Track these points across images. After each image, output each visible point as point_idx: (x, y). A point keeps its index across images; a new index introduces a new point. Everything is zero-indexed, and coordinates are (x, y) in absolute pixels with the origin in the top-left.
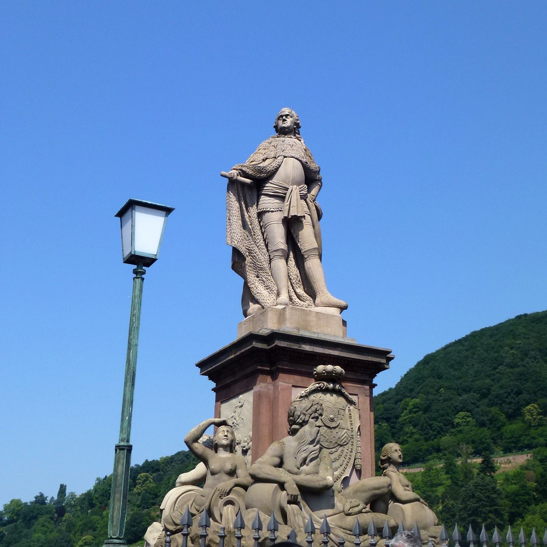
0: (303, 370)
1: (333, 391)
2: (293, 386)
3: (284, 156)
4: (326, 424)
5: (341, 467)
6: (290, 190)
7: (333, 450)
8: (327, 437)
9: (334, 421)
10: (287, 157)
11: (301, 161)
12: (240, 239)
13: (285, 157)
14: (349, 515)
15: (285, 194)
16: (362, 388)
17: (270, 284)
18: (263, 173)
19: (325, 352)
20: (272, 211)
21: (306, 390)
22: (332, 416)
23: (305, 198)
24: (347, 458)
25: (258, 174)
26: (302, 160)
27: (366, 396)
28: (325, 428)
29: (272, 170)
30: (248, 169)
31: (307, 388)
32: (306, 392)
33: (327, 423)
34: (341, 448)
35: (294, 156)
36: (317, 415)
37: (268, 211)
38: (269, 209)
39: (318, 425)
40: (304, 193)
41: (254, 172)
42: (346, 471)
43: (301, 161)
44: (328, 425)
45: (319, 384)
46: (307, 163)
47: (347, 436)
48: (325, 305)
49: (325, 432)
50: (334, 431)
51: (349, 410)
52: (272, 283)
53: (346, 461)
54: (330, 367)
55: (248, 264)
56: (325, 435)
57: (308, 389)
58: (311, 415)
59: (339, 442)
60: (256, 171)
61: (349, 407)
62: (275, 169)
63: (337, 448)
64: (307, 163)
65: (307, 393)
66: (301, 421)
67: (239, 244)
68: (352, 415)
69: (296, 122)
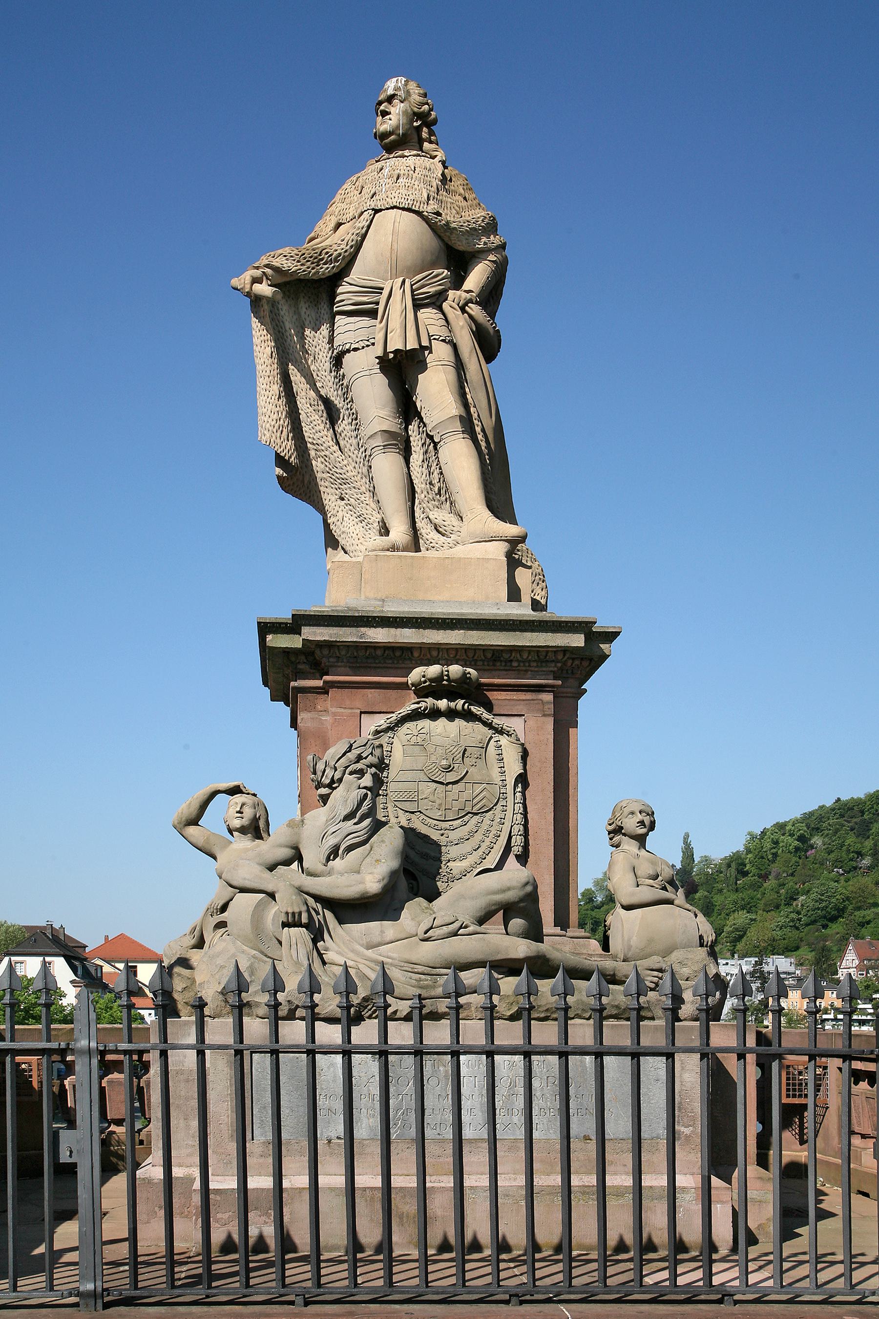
1: (451, 714)
12: (277, 426)
15: (377, 303)
16: (535, 702)
17: (364, 511)
18: (325, 264)
20: (356, 350)
25: (313, 268)
27: (544, 715)
37: (348, 351)
38: (347, 346)
41: (302, 265)
66: (327, 781)
67: (274, 437)
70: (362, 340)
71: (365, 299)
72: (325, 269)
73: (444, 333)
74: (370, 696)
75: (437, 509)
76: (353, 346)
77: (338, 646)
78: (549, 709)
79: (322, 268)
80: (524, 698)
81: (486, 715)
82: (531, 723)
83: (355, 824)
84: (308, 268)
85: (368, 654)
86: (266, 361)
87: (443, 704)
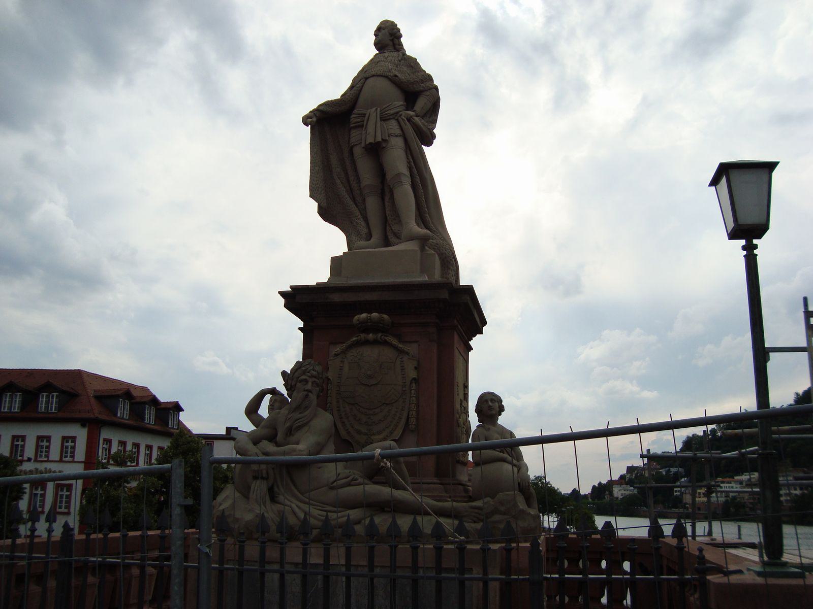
1: (375, 342)
3: (365, 78)
4: (363, 382)
6: (367, 116)
11: (386, 77)
13: (366, 79)
14: (332, 488)
15: (363, 121)
20: (356, 145)
22: (369, 373)
31: (344, 343)
36: (303, 377)
39: (306, 389)
40: (391, 112)
43: (386, 77)
45: (357, 337)
46: (396, 76)
54: (364, 315)
58: (299, 377)
69: (390, 32)
71: (359, 120)
73: (398, 132)
76: (355, 143)
81: (395, 342)
83: (300, 413)
87: (371, 336)
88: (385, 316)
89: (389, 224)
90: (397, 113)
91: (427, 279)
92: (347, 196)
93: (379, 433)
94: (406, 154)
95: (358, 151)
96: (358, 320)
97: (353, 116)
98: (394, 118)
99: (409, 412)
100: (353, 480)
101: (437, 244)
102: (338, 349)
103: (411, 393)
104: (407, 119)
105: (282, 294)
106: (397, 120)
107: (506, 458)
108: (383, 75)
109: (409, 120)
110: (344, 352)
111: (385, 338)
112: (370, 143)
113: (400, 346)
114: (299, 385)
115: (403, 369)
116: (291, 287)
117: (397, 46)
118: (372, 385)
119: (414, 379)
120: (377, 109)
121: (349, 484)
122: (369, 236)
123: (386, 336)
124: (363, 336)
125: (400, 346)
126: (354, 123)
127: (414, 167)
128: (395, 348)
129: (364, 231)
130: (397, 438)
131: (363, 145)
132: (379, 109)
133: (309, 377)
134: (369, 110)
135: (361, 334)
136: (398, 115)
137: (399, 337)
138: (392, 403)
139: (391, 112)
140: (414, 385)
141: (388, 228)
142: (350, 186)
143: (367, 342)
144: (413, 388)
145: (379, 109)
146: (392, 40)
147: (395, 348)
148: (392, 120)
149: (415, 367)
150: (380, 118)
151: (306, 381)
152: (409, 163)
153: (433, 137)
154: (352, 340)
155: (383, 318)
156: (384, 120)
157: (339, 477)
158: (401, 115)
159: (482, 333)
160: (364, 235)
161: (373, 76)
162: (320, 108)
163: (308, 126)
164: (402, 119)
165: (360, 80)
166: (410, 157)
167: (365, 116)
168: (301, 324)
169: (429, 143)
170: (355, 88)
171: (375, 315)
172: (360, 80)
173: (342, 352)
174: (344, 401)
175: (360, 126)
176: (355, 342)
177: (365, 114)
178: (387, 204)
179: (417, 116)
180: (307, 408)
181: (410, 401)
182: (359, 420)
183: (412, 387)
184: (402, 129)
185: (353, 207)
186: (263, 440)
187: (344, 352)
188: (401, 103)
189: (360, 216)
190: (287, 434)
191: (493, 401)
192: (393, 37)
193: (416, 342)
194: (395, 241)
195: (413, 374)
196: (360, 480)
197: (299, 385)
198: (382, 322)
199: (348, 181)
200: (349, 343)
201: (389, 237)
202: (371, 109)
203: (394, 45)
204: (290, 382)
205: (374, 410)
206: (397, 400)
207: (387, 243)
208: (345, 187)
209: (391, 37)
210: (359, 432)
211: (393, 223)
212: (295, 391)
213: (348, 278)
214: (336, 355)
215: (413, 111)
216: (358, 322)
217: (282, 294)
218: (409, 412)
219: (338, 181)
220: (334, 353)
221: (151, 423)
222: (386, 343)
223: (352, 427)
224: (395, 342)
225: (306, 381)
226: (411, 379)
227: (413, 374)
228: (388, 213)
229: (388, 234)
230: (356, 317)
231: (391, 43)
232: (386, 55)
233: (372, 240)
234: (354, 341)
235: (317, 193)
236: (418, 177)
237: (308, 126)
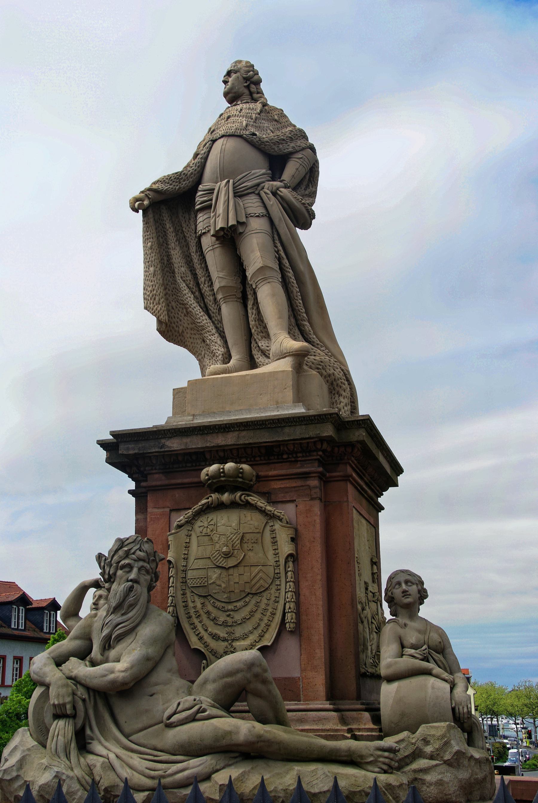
0: (186, 481)
1: (234, 505)
2: (171, 511)
3: (211, 140)
4: (217, 564)
5: (255, 632)
7: (239, 604)
8: (223, 585)
9: (231, 556)
10: (216, 140)
11: (240, 136)
12: (151, 295)
13: (214, 141)
14: (170, 726)
15: (211, 200)
16: (305, 488)
18: (184, 181)
19: (208, 445)
20: (204, 233)
21: (186, 514)
22: (225, 549)
23: (257, 192)
24: (268, 614)
25: (177, 186)
26: (242, 133)
27: (312, 499)
28: (218, 571)
29: (195, 170)
30: (162, 183)
31: (190, 509)
32: (186, 516)
33: (219, 562)
34: (257, 598)
35: (225, 134)
36: (127, 561)
39: (130, 578)
41: (171, 185)
42: (267, 636)
43: (240, 136)
44: (220, 565)
45: (208, 498)
46: (254, 134)
47: (264, 576)
48: (278, 357)
49: (219, 578)
50: (235, 573)
51: (273, 531)
52: (216, 345)
53: (265, 620)
54: (214, 467)
55: (188, 327)
56: (218, 582)
57: (190, 512)
59: (248, 590)
60: (174, 182)
61: (272, 526)
62: (198, 167)
63: (247, 599)
64: (255, 135)
65: (188, 518)
68: (278, 539)
69: (244, 76)
70: (207, 227)
71: (205, 199)
72: (185, 184)
73: (261, 210)
74: (177, 495)
75: (264, 339)
76: (203, 231)
77: (150, 457)
78: (315, 493)
79: (182, 184)
80: (294, 485)
82: (301, 507)
83: (123, 615)
84: (174, 186)
85: (172, 460)
86: (148, 252)
87: (226, 497)
88: (246, 467)
89: (255, 340)
90: (258, 185)
91: (303, 410)
92: (195, 305)
93: (245, 637)
94: (274, 240)
95: (207, 242)
96: (207, 475)
97: (199, 193)
98: (253, 193)
99: (285, 604)
100: (198, 712)
101: (321, 362)
102: (181, 518)
103: (286, 577)
104: (272, 193)
105: (103, 444)
106: (259, 195)
107: (431, 670)
108: (236, 134)
109: (274, 194)
110: (190, 522)
111: (246, 498)
112: (222, 229)
113: (269, 508)
114: (120, 572)
115: (274, 542)
116: (113, 434)
117: (255, 96)
118: (230, 568)
119: (291, 555)
120: (228, 182)
121: (193, 719)
122: (227, 357)
123: (248, 495)
124: (214, 496)
125: (269, 508)
126: (199, 204)
127: (285, 257)
128: (263, 512)
129: (220, 351)
130: (269, 644)
131: (212, 232)
132: (231, 181)
133: (135, 560)
134: (219, 184)
135: (212, 495)
136: (260, 188)
137: (267, 496)
138: (261, 592)
139: (249, 184)
140: (291, 564)
141: (253, 344)
142: (200, 290)
143: (220, 506)
144: (289, 569)
145: (231, 181)
146: (248, 87)
147: (263, 512)
148: (250, 195)
149: (291, 538)
150: (234, 193)
151: (130, 567)
152: (277, 252)
153: (312, 216)
154: (200, 504)
155: (241, 469)
156: (241, 196)
157: (180, 708)
158: (263, 188)
159: (396, 485)
160: (220, 357)
161: (223, 136)
162: (155, 187)
163: (138, 212)
164: (265, 193)
165: (206, 144)
166: (279, 245)
167: (213, 193)
168: (132, 485)
169: (306, 226)
170: (199, 156)
171: (229, 465)
172: (206, 144)
173: (187, 522)
174: (192, 592)
175: (207, 208)
176: (204, 508)
177: (214, 189)
178: (250, 311)
179: (286, 187)
180: (132, 606)
181: (286, 589)
182: (215, 618)
183: (289, 567)
184: (265, 207)
185: (204, 320)
186: (71, 658)
187: (190, 522)
188: (263, 171)
189: (214, 331)
190: (105, 647)
191: (409, 584)
192: (248, 83)
193: (292, 501)
194: (263, 361)
195: (286, 548)
196: (211, 711)
197: (120, 572)
198: (240, 475)
199: (198, 285)
200: (197, 507)
201: (255, 357)
202: (221, 181)
203: (251, 94)
204: (107, 570)
205: (235, 604)
206: (267, 589)
207: (253, 364)
208: (193, 293)
209: (246, 82)
210: (215, 637)
211: (260, 337)
212: (115, 583)
213: (194, 415)
214: (179, 526)
215: (281, 181)
216: (207, 477)
217: (103, 444)
218: (285, 604)
219: (183, 285)
220: (175, 524)
221: (20, 628)
222: (248, 505)
223: (206, 630)
224: (261, 503)
225: (130, 567)
226: (286, 556)
227: (286, 548)
228: (252, 323)
229: (254, 352)
230: (205, 471)
231: (246, 91)
232: (239, 107)
233: (232, 362)
234: (203, 505)
235: (153, 303)
236: (291, 271)
237: (138, 212)
